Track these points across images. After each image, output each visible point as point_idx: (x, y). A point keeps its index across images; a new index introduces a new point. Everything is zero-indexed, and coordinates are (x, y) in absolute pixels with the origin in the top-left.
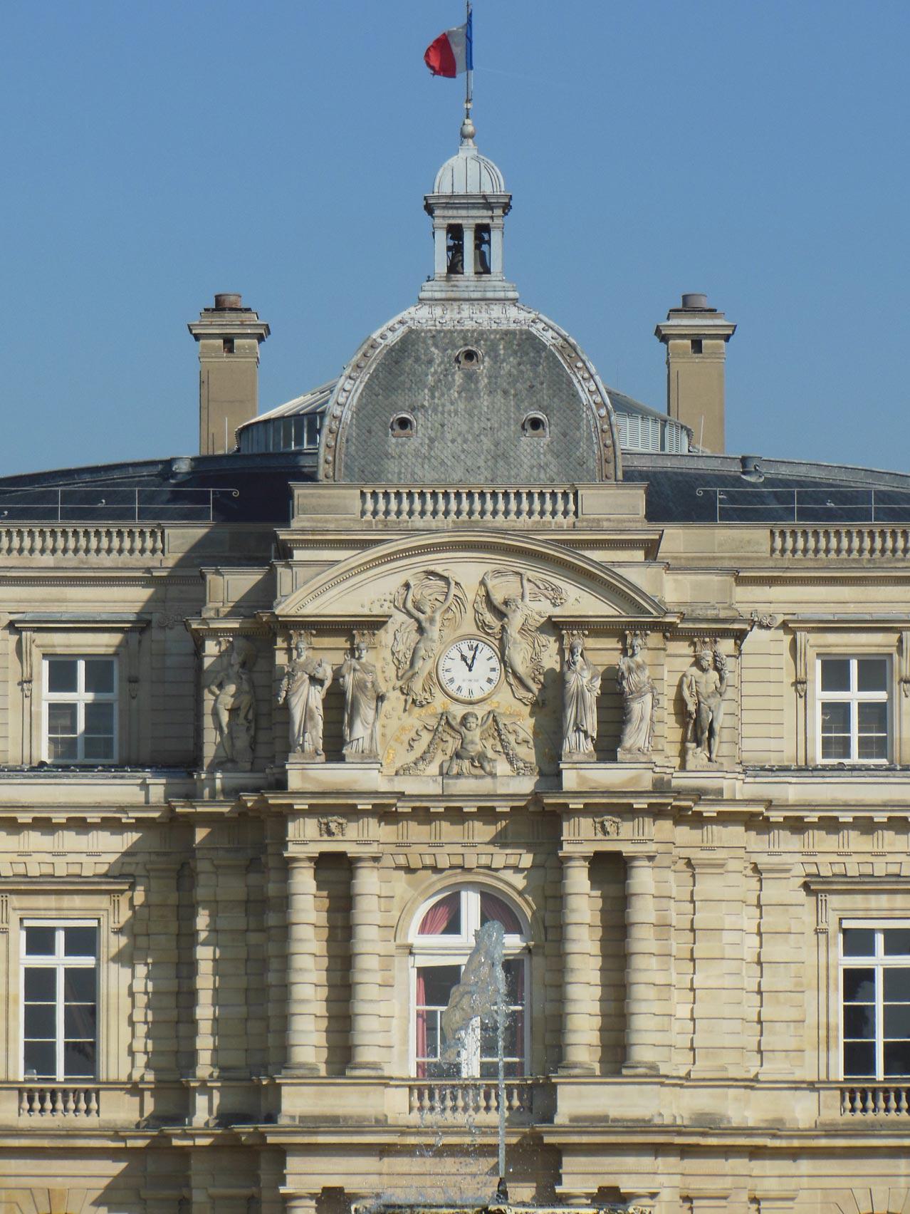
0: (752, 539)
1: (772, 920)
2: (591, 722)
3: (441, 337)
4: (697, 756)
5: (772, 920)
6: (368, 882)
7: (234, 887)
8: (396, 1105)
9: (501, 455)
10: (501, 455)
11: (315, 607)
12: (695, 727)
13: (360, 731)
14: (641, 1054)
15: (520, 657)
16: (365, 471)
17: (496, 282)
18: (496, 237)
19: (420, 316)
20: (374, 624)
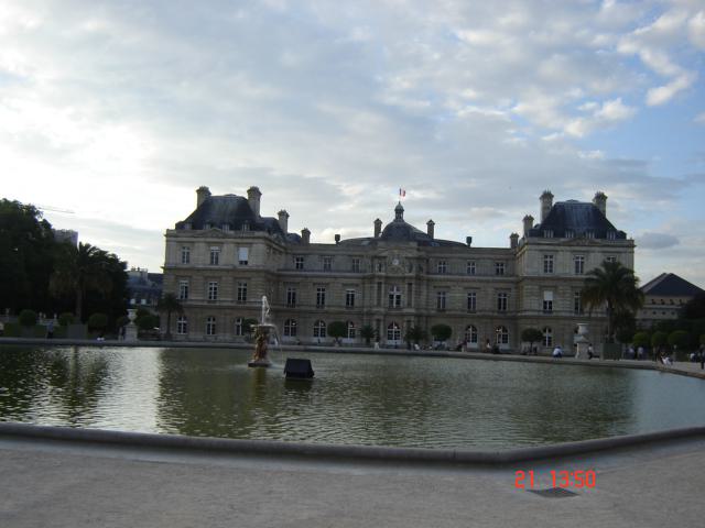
12: (421, 269)
13: (383, 269)
20: (385, 257)
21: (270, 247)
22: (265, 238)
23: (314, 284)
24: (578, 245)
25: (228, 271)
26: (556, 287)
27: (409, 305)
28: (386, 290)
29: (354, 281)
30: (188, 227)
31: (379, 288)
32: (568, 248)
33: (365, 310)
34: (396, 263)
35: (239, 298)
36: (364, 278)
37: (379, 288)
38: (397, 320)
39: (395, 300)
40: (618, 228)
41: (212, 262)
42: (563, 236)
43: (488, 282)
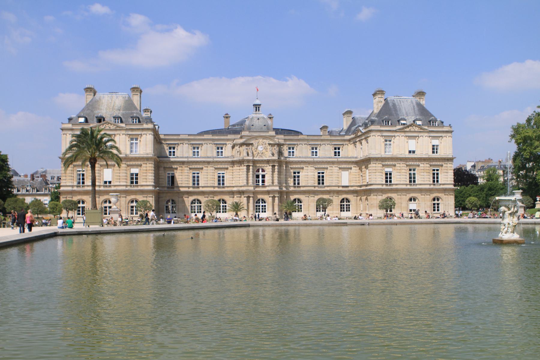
3: (256, 117)
7: (238, 168)
10: (261, 128)
12: (280, 153)
13: (250, 154)
16: (249, 129)
17: (260, 112)
20: (252, 144)
21: (154, 135)
24: (410, 131)
26: (395, 166)
28: (253, 172)
30: (82, 120)
31: (248, 169)
32: (403, 134)
33: (235, 189)
34: (260, 148)
35: (132, 183)
36: (233, 163)
37: (248, 169)
38: (265, 197)
39: (261, 179)
43: (333, 163)
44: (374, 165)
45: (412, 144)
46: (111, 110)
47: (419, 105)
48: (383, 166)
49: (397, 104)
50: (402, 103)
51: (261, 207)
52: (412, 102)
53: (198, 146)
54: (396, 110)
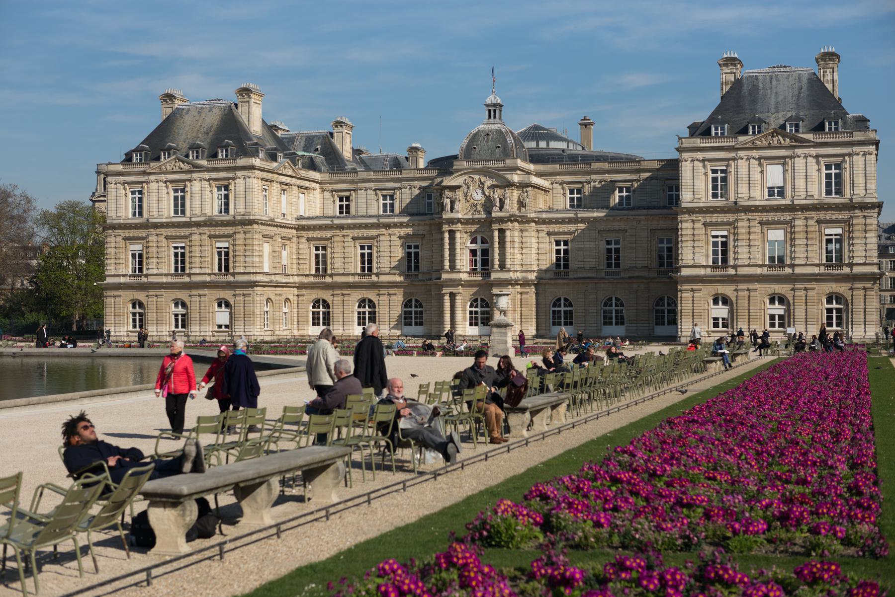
0: (556, 167)
1: (541, 240)
2: (498, 204)
4: (523, 209)
5: (541, 240)
6: (458, 235)
8: (464, 277)
9: (492, 153)
10: (492, 153)
11: (449, 184)
13: (457, 206)
14: (508, 266)
15: (487, 192)
17: (497, 120)
18: (497, 112)
19: (482, 127)
22: (252, 168)
23: (354, 239)
24: (770, 147)
25: (198, 225)
27: (502, 265)
29: (421, 230)
34: (478, 197)
40: (853, 111)
41: (176, 212)
42: (744, 132)
44: (685, 225)
45: (774, 175)
46: (195, 134)
47: (816, 83)
48: (705, 225)
49: (761, 85)
50: (774, 83)
51: (479, 316)
52: (800, 79)
53: (391, 192)
54: (754, 101)
